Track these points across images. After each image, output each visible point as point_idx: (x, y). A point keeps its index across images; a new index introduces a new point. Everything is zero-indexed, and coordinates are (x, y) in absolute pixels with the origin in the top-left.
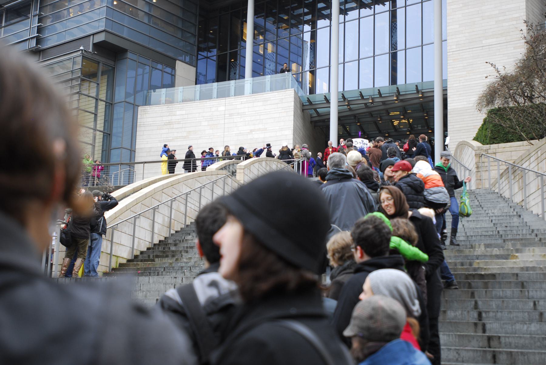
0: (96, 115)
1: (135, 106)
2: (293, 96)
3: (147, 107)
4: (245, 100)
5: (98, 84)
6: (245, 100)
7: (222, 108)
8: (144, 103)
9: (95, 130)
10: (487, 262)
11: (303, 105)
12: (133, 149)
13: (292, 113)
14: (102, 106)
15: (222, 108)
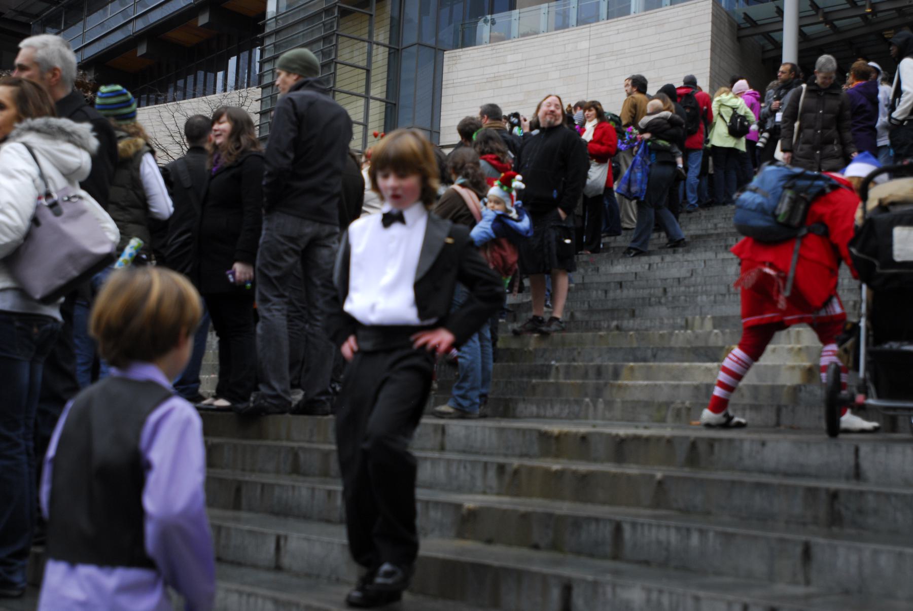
0: (368, 71)
1: (437, 53)
2: (710, 11)
3: (458, 52)
4: (624, 26)
5: (371, 15)
6: (624, 26)
7: (584, 45)
8: (460, 43)
9: (367, 97)
10: (650, 367)
11: (740, 28)
12: (435, 129)
13: (708, 45)
14: (381, 56)
15: (584, 45)
